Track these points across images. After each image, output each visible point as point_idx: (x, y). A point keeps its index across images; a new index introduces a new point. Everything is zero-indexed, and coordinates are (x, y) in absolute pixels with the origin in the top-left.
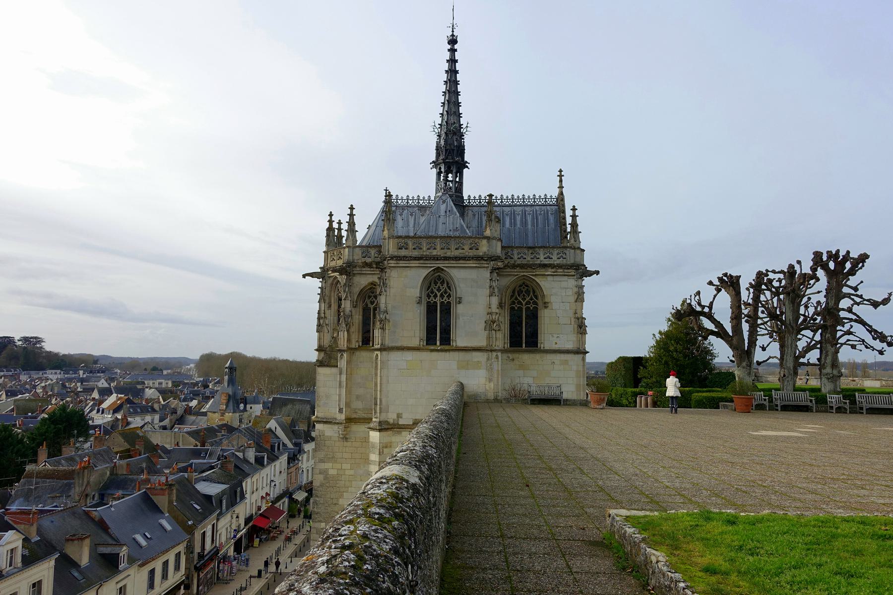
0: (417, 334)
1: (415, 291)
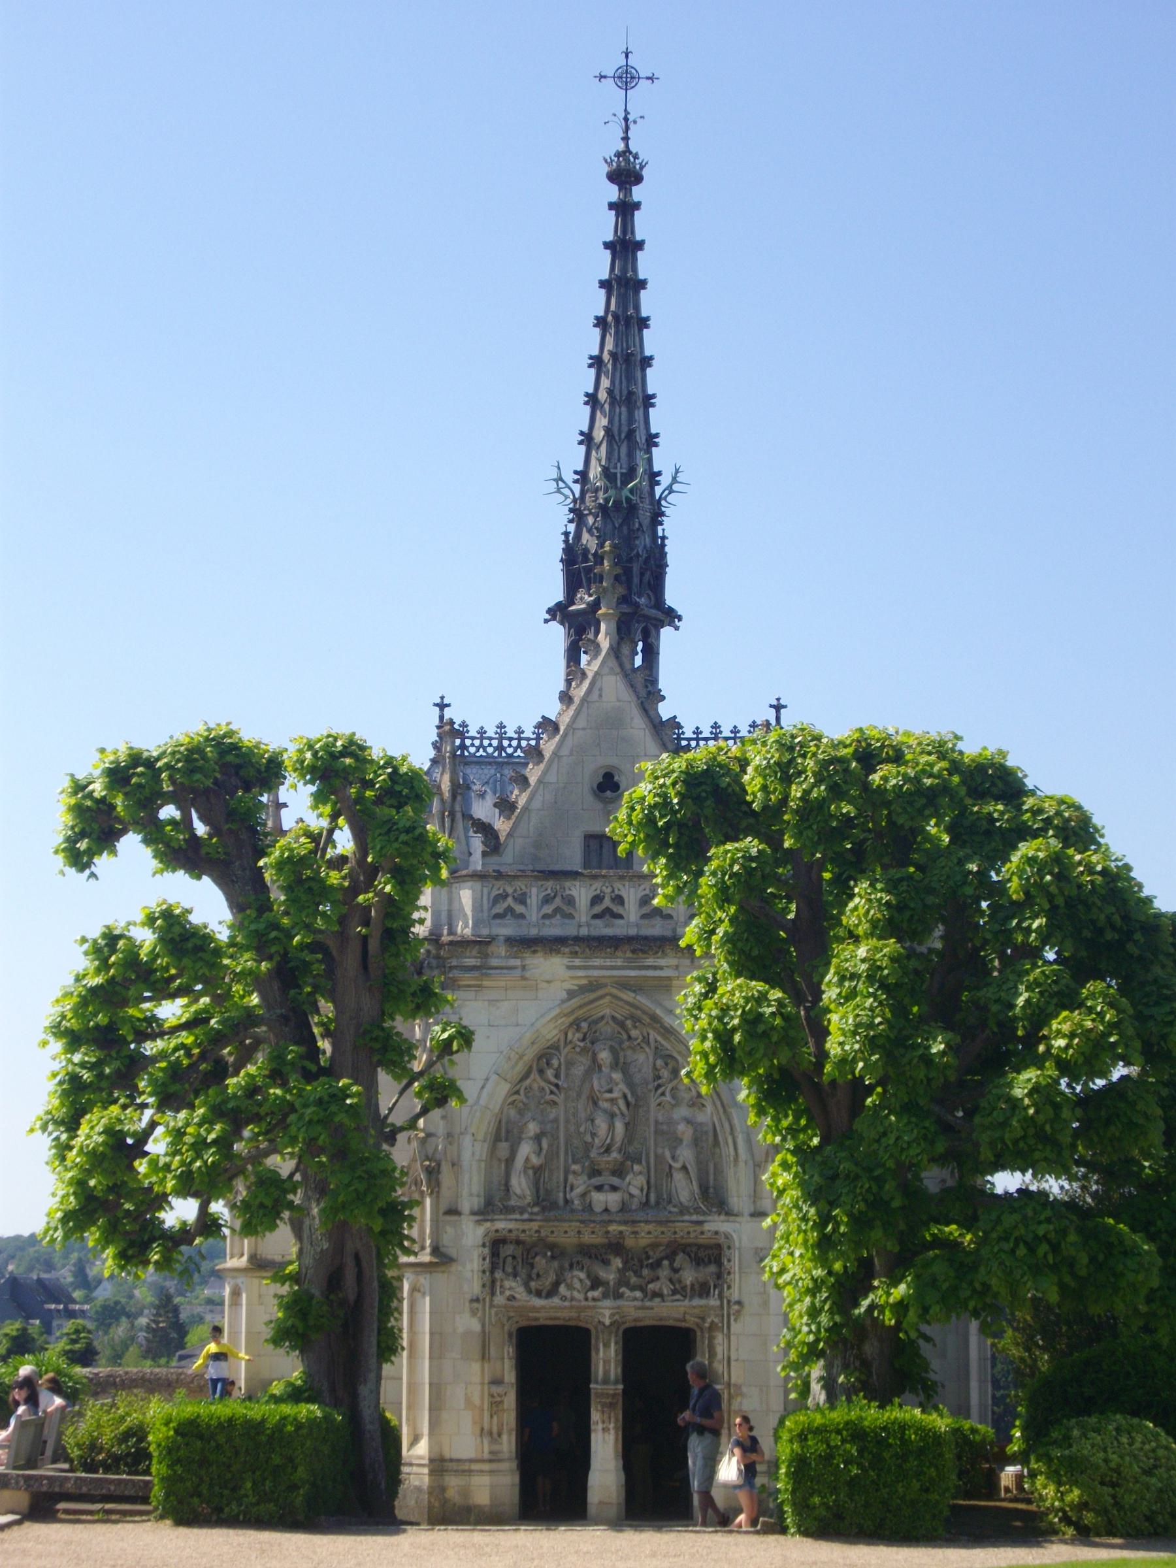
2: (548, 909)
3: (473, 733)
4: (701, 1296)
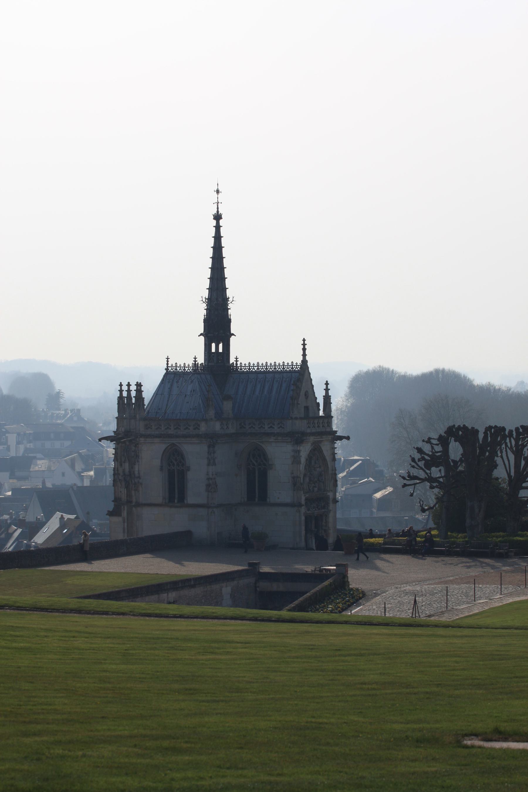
1: (157, 462)
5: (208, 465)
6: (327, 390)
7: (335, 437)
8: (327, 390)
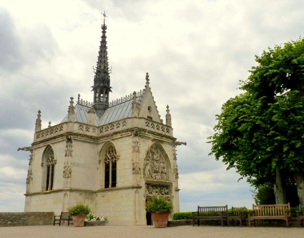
0: (41, 185)
2: (152, 126)
3: (83, 101)
4: (167, 195)
5: (66, 155)
6: (168, 111)
7: (174, 142)
8: (168, 111)
